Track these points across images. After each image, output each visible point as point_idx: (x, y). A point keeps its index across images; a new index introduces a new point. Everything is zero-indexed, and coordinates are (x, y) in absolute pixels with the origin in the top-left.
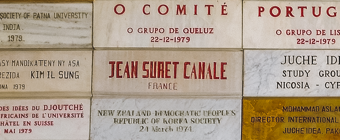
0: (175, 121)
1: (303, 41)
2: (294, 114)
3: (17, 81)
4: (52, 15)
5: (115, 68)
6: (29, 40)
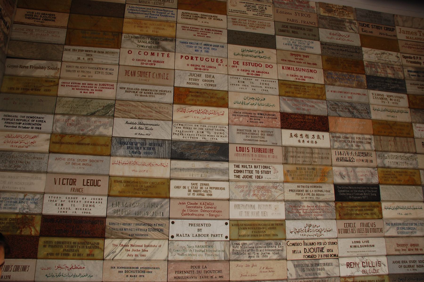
0: (148, 93)
1: (197, 69)
2: (193, 94)
3: (90, 75)
4: (105, 52)
5: (127, 72)
6: (95, 60)
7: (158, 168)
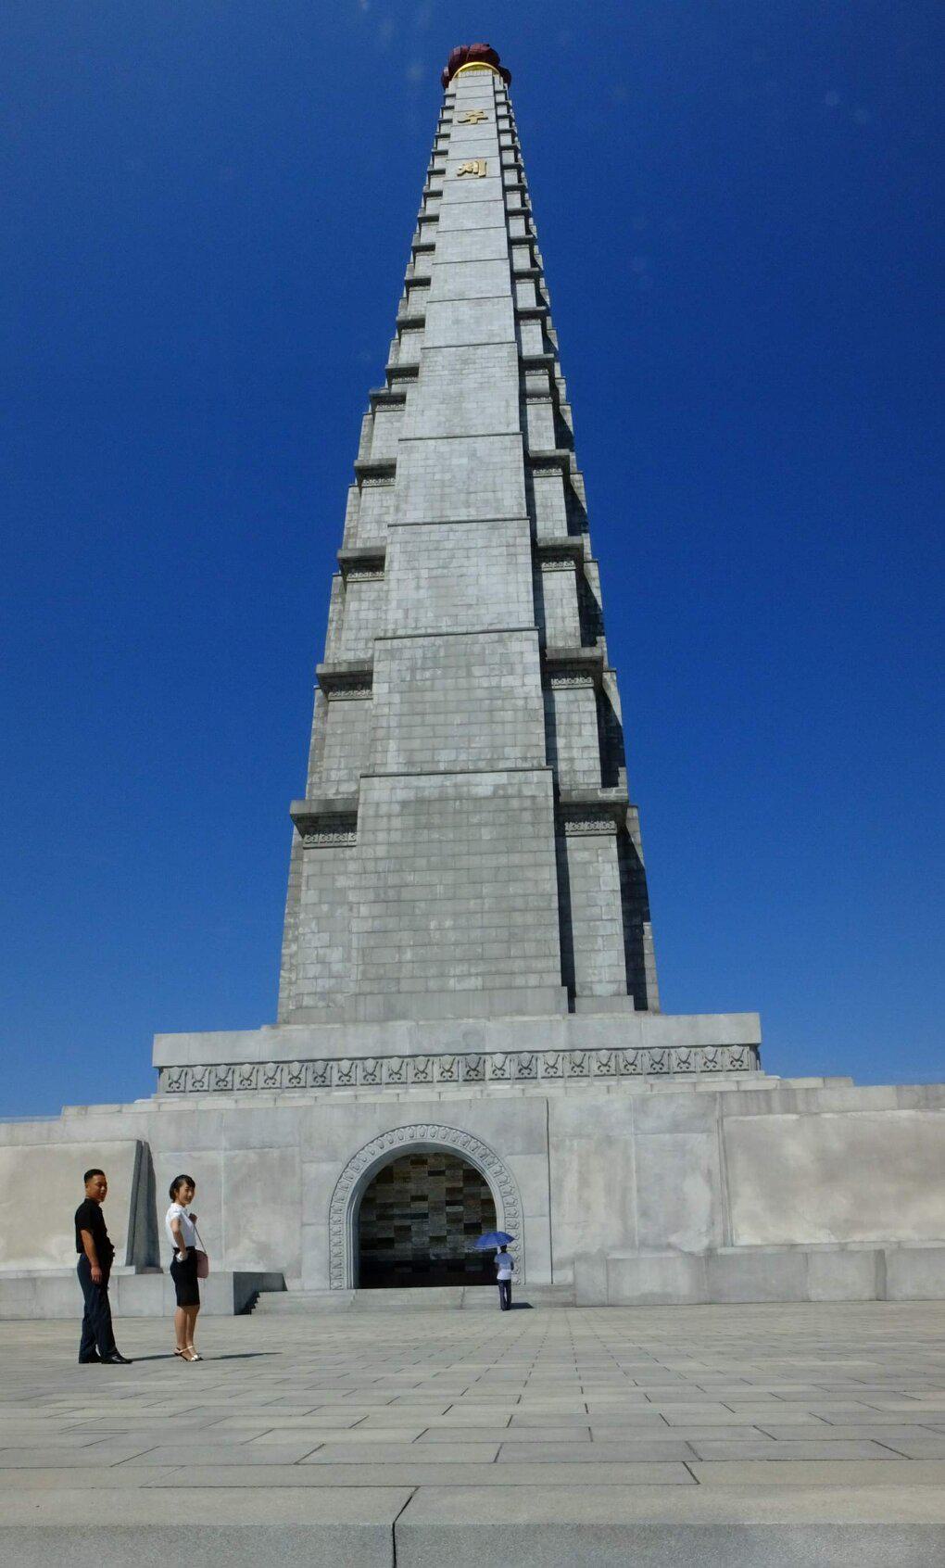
7: (408, 1222)
